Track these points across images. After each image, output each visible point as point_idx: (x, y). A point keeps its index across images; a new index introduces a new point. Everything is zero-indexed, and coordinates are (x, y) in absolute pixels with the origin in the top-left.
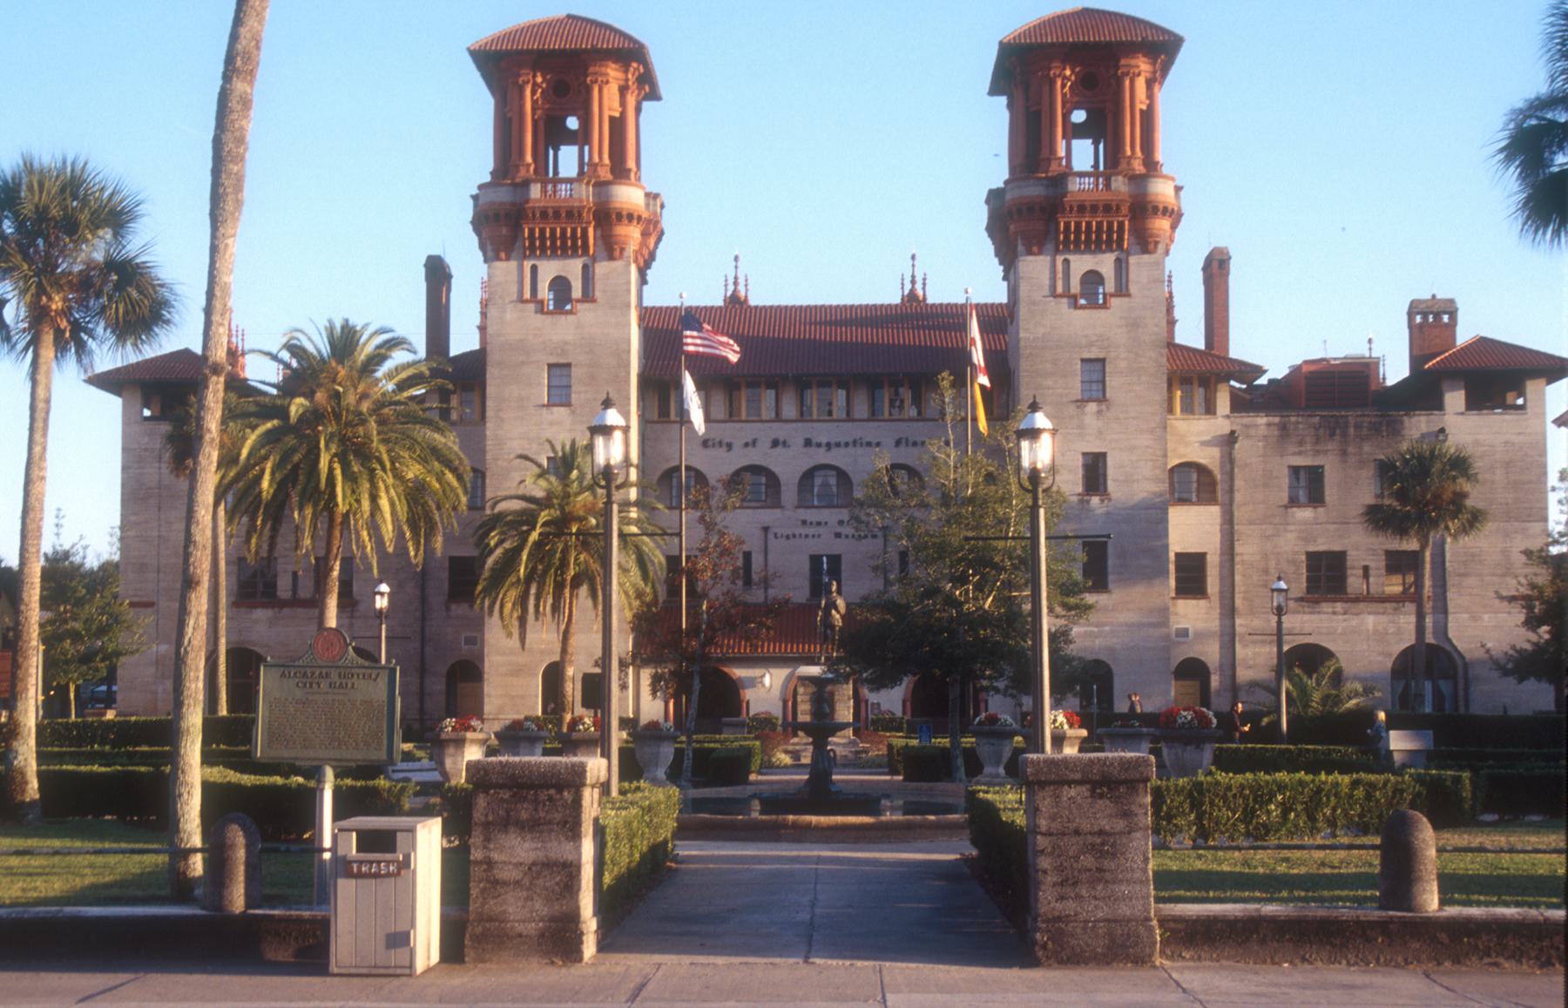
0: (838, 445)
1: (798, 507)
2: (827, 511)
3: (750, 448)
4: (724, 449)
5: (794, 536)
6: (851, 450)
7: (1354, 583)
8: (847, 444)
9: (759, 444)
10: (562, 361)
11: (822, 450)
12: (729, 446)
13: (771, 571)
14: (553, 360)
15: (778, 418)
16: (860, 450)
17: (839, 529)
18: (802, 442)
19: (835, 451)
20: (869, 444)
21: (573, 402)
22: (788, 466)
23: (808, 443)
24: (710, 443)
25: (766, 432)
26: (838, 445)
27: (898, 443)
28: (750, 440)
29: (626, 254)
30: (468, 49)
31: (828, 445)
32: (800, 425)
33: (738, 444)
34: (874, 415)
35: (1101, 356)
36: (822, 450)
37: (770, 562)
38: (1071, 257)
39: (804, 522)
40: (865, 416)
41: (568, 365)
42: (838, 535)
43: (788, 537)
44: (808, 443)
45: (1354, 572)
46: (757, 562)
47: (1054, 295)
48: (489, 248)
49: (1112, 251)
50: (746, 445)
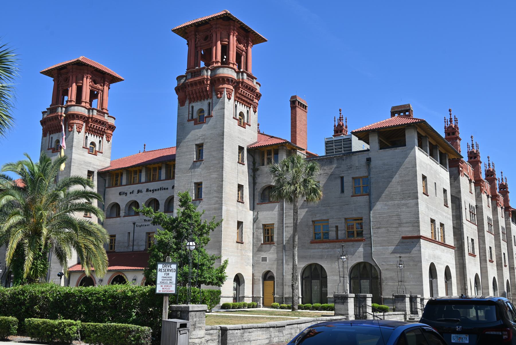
0: (156, 190)
3: (132, 194)
4: (125, 195)
5: (142, 226)
7: (332, 235)
8: (158, 189)
9: (134, 192)
12: (126, 194)
13: (135, 239)
15: (140, 182)
19: (155, 192)
20: (165, 189)
22: (142, 199)
23: (147, 190)
24: (121, 194)
25: (135, 187)
26: (156, 190)
28: (132, 191)
29: (73, 129)
31: (153, 190)
33: (128, 193)
35: (202, 142)
36: (152, 192)
37: (135, 237)
38: (193, 104)
39: (145, 220)
43: (140, 226)
45: (332, 229)
46: (132, 235)
47: (189, 120)
49: (207, 99)
50: (131, 193)
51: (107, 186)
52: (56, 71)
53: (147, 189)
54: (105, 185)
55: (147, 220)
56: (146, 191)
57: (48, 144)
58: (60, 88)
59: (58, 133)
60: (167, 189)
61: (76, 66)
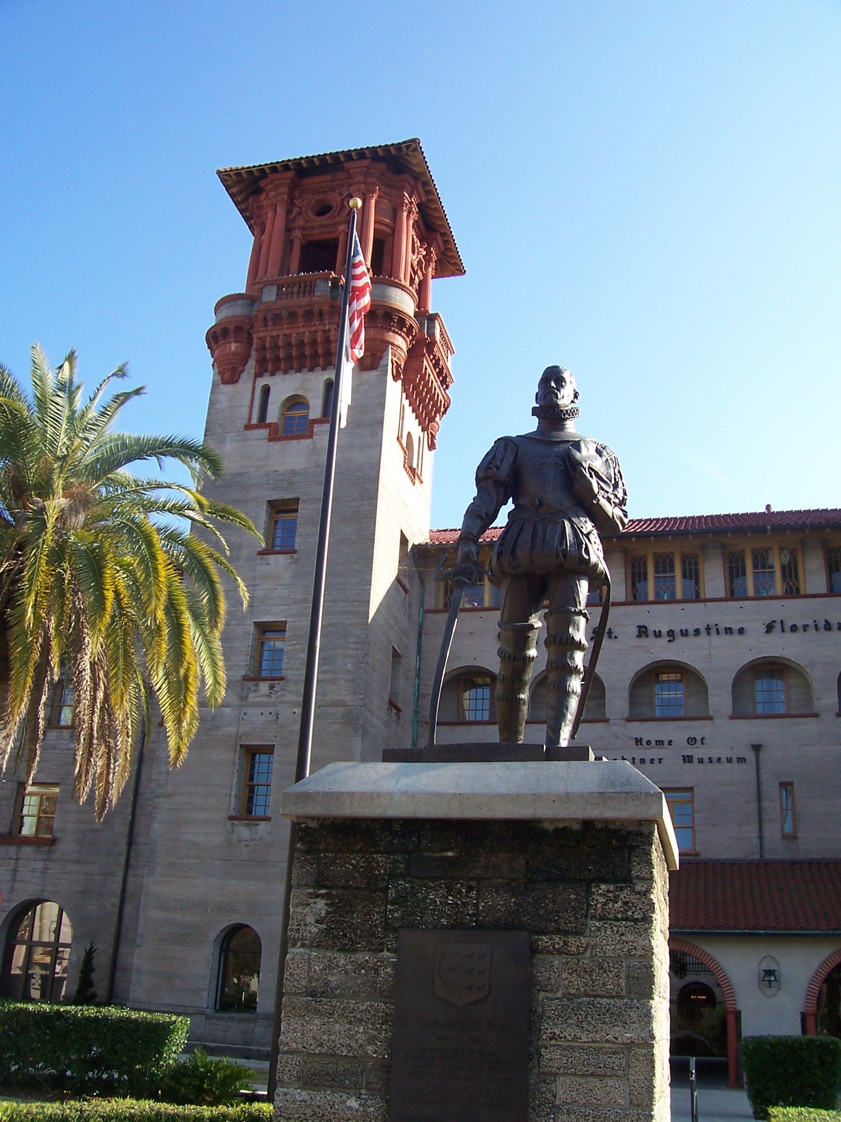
0: (684, 633)
1: (628, 720)
2: (671, 725)
6: (703, 639)
8: (697, 632)
10: (287, 496)
11: (663, 641)
14: (275, 496)
16: (715, 640)
17: (689, 751)
18: (635, 631)
19: (680, 641)
20: (729, 631)
21: (296, 547)
23: (642, 631)
26: (684, 633)
27: (770, 628)
29: (382, 363)
30: (219, 173)
31: (671, 633)
32: (630, 608)
34: (733, 594)
39: (638, 741)
40: (722, 594)
41: (297, 500)
42: (688, 759)
44: (642, 631)
48: (217, 370)
51: (430, 603)
52: (291, 174)
53: (640, 627)
54: (422, 603)
55: (649, 742)
56: (639, 636)
57: (245, 411)
58: (298, 233)
59: (299, 370)
60: (741, 631)
61: (382, 166)
